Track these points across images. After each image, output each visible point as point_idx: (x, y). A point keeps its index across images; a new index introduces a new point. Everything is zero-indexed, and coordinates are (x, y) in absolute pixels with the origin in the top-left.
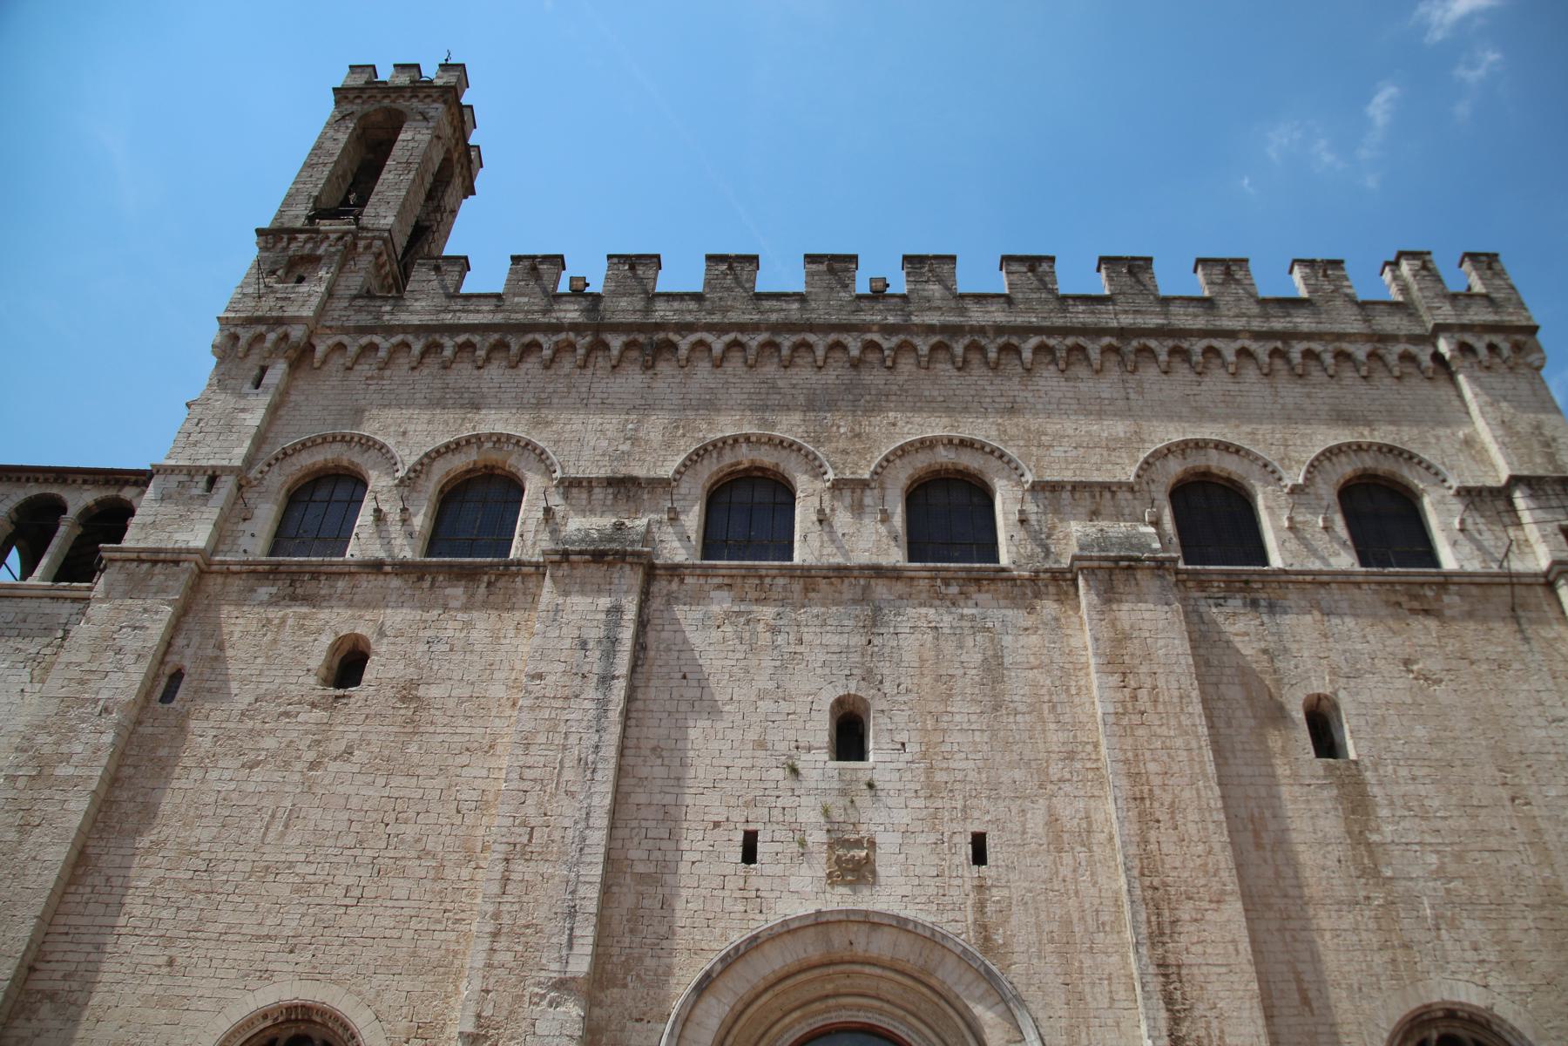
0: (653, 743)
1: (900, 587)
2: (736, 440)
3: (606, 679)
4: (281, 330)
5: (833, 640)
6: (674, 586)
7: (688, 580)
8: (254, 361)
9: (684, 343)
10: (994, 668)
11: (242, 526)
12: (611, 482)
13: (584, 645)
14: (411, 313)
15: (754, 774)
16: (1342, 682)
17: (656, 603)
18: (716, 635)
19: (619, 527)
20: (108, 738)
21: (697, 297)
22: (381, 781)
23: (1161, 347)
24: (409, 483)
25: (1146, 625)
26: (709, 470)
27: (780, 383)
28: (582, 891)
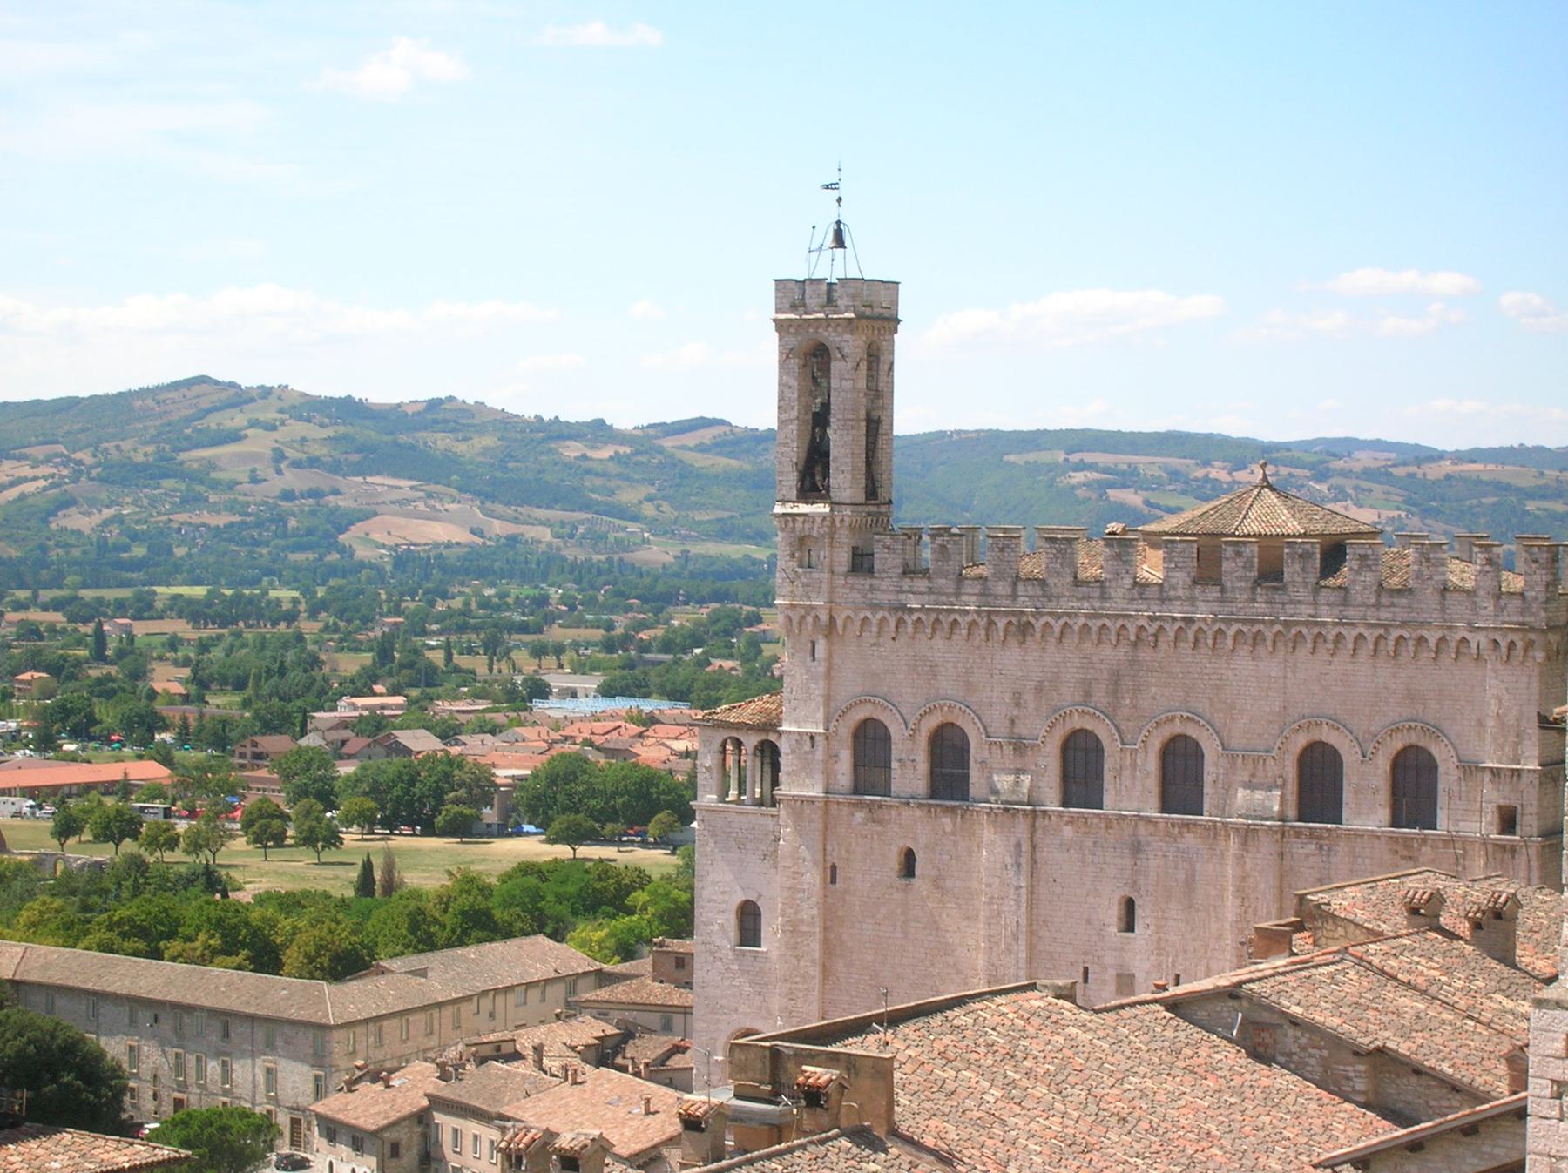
1: (1151, 828)
5: (1118, 861)
10: (1190, 881)
17: (1039, 834)
20: (815, 912)
27: (1095, 659)
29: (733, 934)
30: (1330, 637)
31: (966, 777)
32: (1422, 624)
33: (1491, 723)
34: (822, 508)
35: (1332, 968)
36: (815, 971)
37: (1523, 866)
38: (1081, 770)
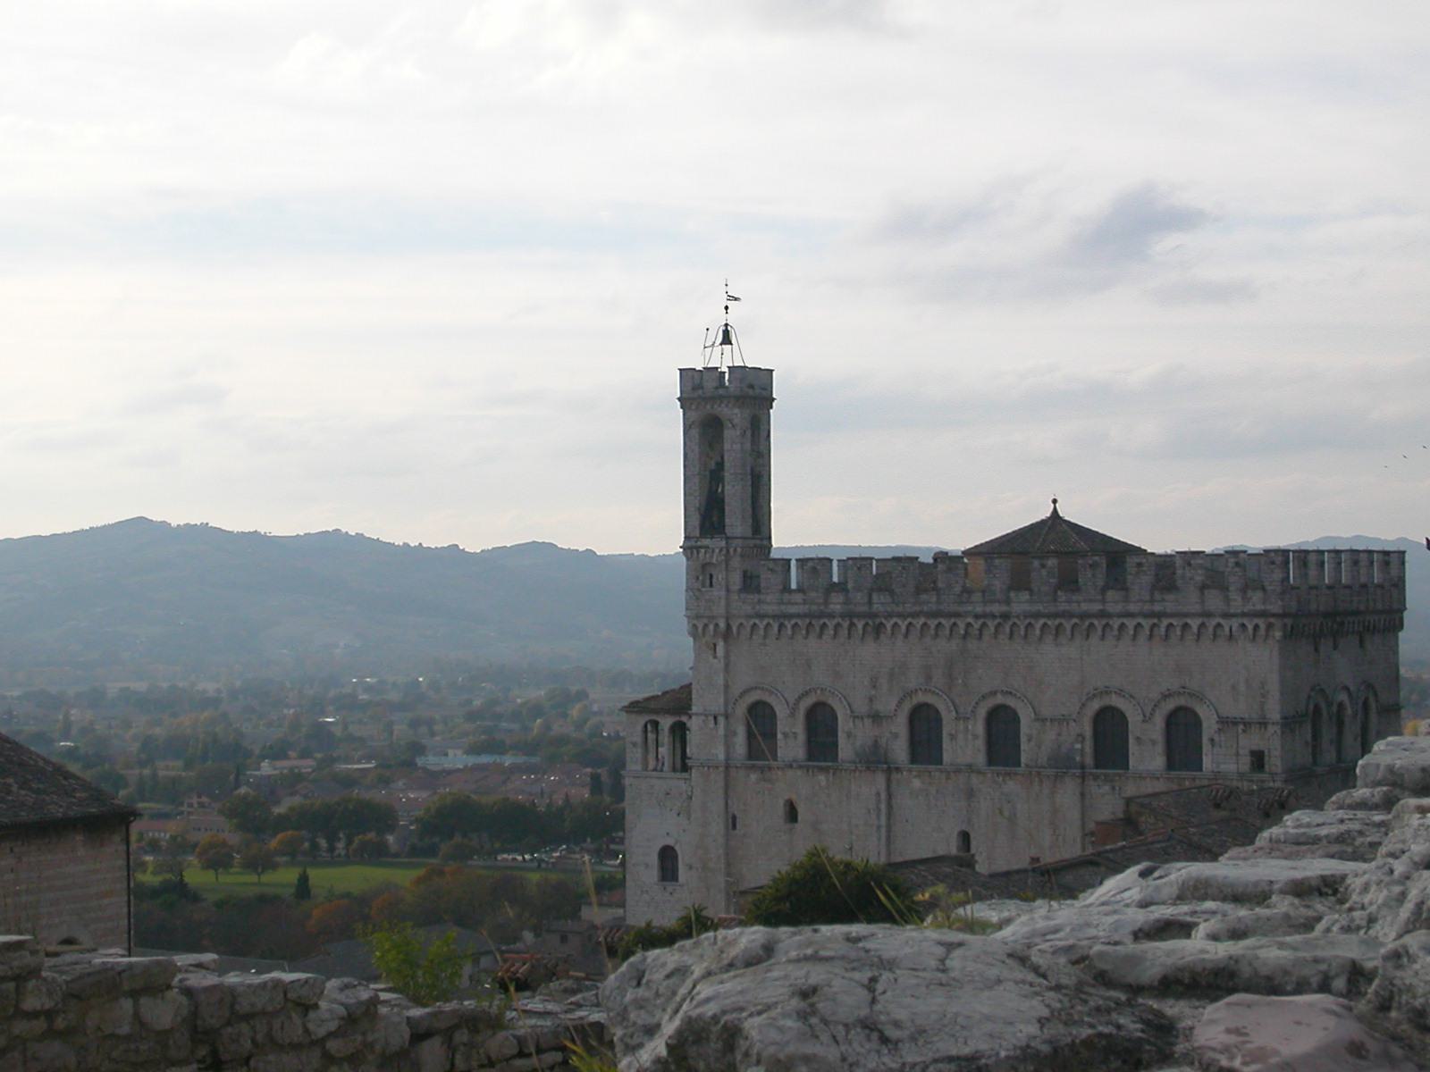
2: (916, 690)
3: (879, 827)
4: (715, 622)
6: (899, 776)
13: (869, 812)
19: (876, 741)
24: (792, 715)
29: (654, 873)
30: (1116, 627)
31: (835, 744)
32: (1186, 615)
33: (1242, 688)
34: (718, 543)
35: (1164, 845)
38: (925, 733)
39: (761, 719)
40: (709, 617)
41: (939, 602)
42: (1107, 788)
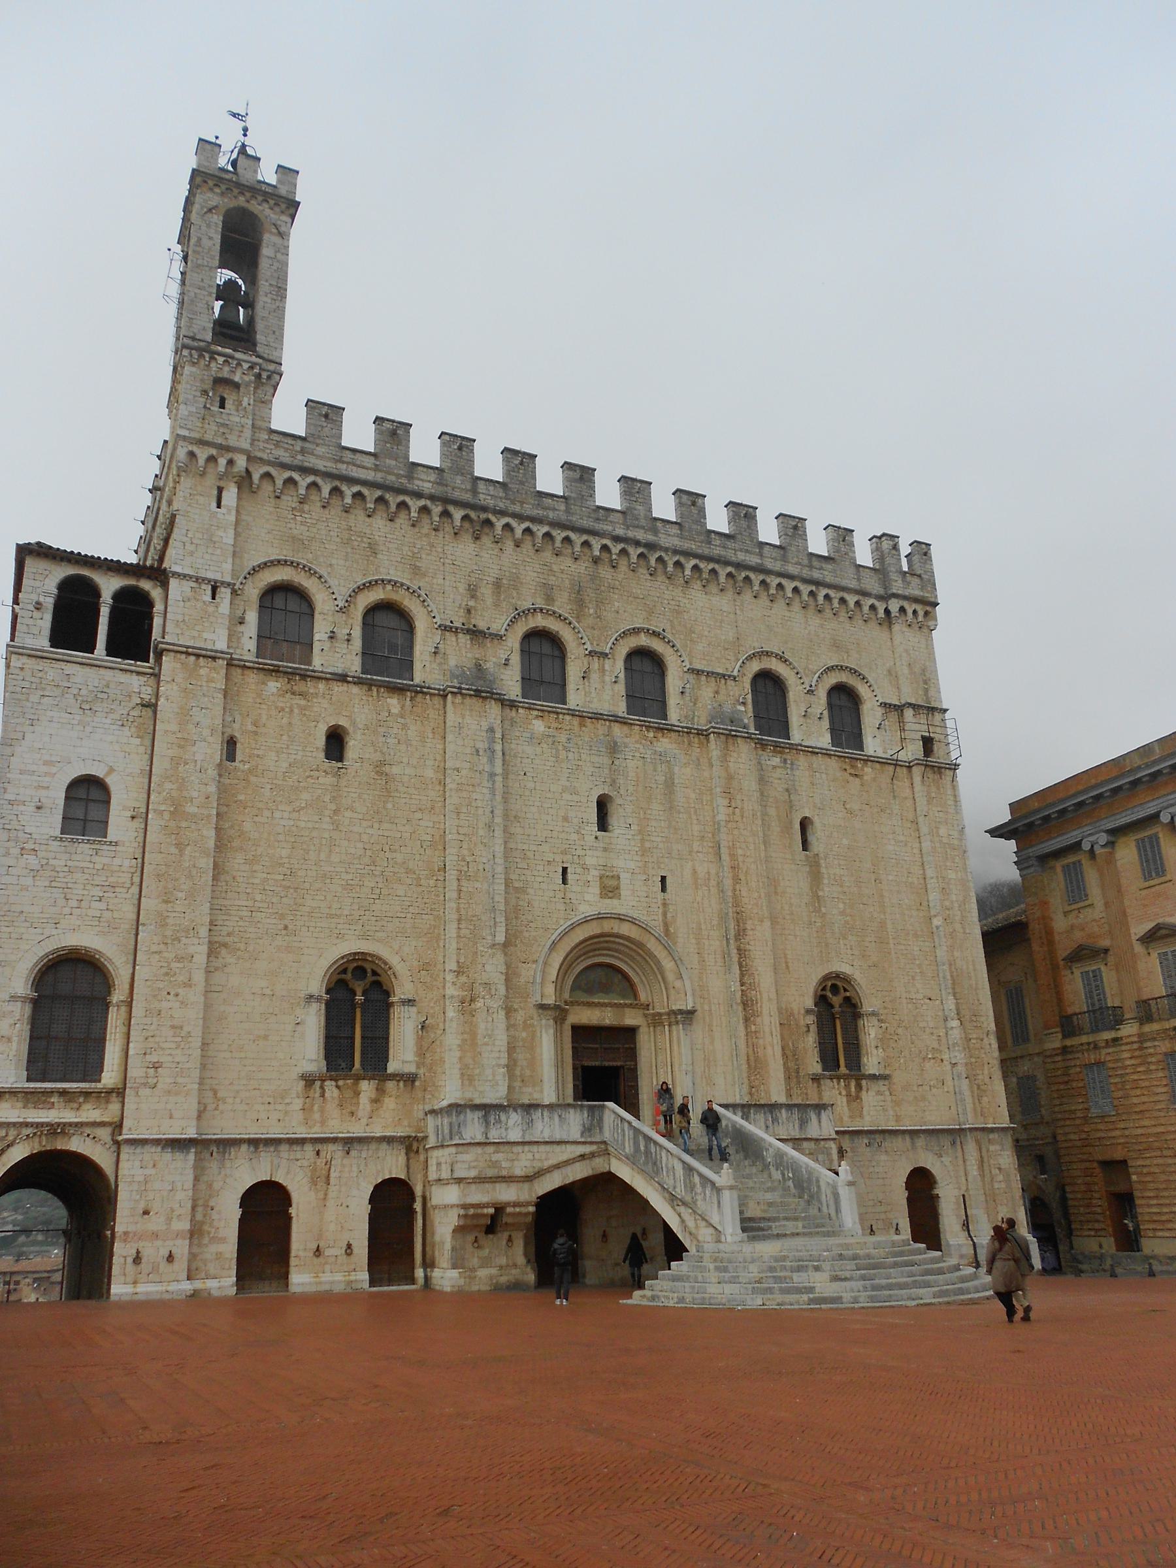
0: (514, 813)
1: (626, 728)
3: (492, 775)
4: (230, 455)
5: (595, 759)
6: (514, 713)
7: (521, 710)
8: (211, 481)
9: (499, 523)
10: (670, 784)
11: (241, 628)
12: (468, 631)
13: (477, 751)
14: (318, 457)
15: (563, 836)
16: (817, 811)
18: (539, 750)
19: (478, 667)
21: (503, 485)
22: (376, 825)
23: (756, 578)
25: (741, 772)
26: (521, 629)
27: (555, 568)
28: (497, 898)
33: (906, 671)
36: (206, 863)
37: (949, 786)
39: (285, 607)
40: (220, 447)
41: (567, 511)
42: (776, 761)
